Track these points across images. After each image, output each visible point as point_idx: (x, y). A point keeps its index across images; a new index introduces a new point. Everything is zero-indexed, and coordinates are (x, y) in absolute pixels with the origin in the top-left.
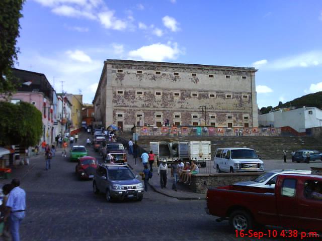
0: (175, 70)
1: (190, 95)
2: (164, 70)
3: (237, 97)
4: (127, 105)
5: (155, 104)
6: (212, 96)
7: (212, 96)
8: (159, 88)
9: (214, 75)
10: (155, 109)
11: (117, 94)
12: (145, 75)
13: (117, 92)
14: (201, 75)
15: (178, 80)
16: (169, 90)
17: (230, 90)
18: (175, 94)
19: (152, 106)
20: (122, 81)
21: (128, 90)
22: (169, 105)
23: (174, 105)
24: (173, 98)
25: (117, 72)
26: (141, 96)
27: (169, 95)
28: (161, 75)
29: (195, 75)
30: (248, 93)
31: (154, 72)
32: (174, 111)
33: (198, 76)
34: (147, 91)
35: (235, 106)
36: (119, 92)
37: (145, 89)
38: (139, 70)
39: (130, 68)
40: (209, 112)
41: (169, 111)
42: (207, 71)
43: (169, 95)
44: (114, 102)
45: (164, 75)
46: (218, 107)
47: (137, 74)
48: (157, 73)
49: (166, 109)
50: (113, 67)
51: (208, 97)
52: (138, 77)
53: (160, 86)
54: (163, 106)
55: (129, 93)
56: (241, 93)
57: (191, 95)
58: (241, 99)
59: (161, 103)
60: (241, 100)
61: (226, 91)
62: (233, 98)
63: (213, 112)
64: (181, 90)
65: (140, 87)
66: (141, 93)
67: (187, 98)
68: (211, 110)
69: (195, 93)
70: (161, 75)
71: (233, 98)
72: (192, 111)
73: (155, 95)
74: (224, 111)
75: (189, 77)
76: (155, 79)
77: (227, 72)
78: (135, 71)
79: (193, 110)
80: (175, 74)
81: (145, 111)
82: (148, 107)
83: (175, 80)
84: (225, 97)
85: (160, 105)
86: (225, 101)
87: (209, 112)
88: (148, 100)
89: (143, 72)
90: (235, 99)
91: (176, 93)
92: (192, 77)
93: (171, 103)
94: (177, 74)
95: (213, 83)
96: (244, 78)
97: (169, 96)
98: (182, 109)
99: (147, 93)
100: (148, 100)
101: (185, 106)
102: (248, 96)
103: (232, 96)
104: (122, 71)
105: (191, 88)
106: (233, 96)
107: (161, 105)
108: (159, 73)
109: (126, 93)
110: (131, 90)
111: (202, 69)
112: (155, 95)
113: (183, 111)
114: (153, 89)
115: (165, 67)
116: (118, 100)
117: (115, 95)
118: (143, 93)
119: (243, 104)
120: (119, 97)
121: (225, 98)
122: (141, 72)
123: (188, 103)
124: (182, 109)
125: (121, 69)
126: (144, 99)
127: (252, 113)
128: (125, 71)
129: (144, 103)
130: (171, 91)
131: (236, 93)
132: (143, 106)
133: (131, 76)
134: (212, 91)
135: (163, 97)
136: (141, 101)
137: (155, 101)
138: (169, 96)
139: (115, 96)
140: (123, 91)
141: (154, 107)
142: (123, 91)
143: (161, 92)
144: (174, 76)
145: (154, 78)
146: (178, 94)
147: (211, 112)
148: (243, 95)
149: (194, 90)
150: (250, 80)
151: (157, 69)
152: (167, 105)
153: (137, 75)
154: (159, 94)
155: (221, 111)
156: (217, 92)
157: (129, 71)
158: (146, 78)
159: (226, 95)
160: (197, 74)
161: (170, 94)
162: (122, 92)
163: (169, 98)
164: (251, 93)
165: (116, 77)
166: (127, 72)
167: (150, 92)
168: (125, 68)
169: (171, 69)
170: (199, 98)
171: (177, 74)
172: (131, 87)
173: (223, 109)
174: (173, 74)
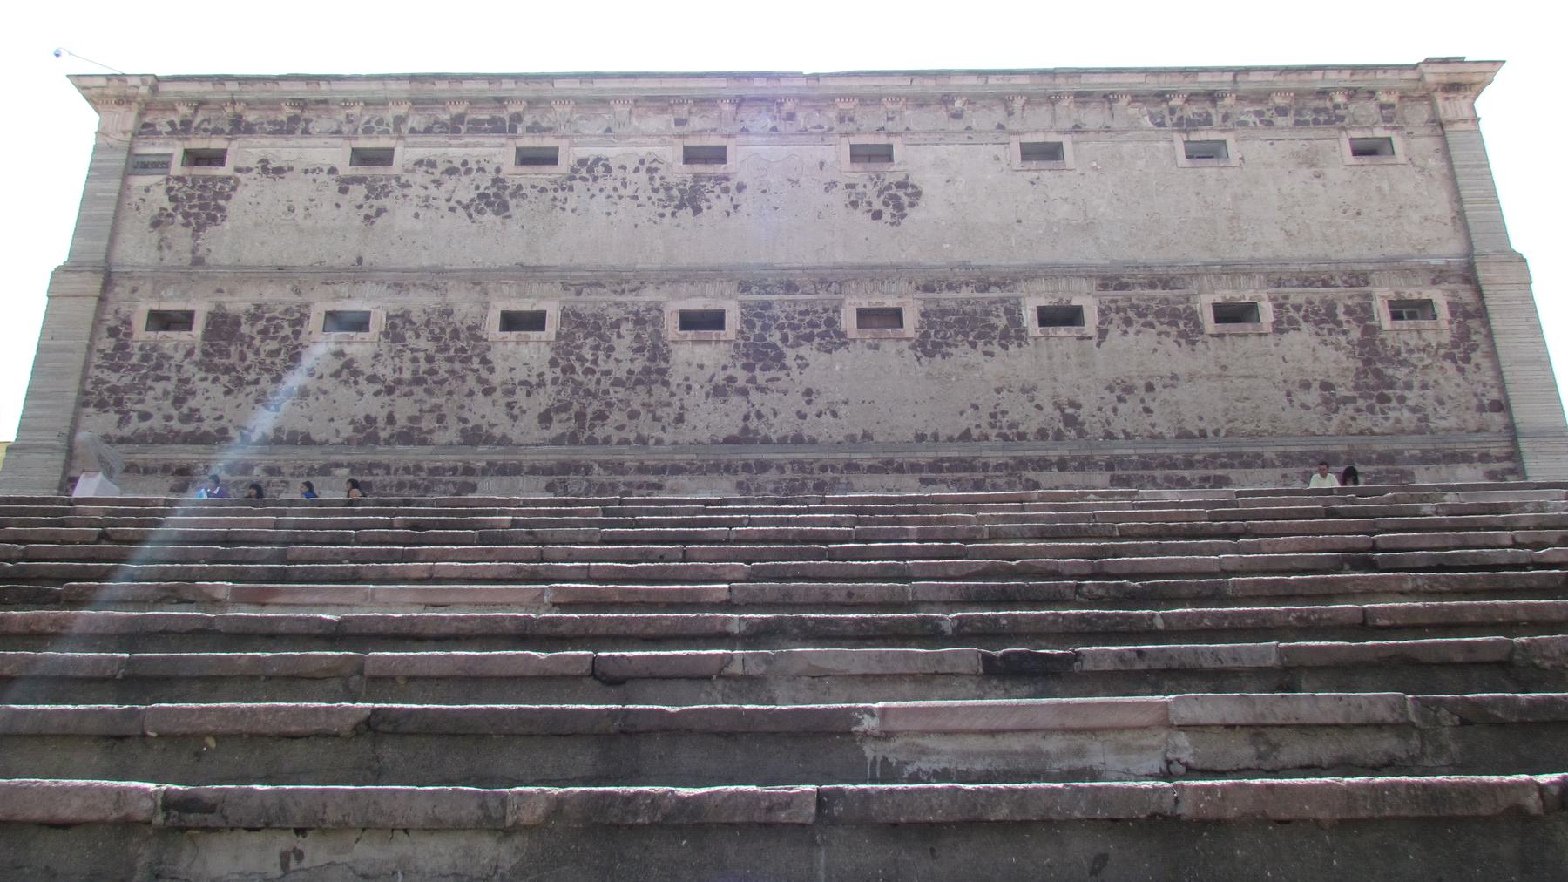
0: (696, 123)
1: (830, 322)
2: (593, 127)
3: (1325, 317)
4: (208, 426)
5: (488, 412)
6: (1060, 316)
7: (1060, 316)
8: (529, 273)
9: (1067, 142)
10: (480, 456)
11: (141, 334)
12: (420, 177)
13: (140, 322)
14: (942, 150)
15: (720, 203)
16: (623, 280)
17: (1243, 253)
18: (690, 321)
19: (452, 434)
20: (212, 230)
21: (239, 303)
22: (616, 417)
23: (668, 414)
24: (658, 352)
25: (177, 169)
26: (360, 347)
27: (626, 328)
28: (563, 167)
29: (885, 154)
30: (1438, 276)
31: (498, 153)
32: (677, 470)
33: (912, 159)
34: (419, 302)
35: (1313, 397)
36: (162, 321)
37: (399, 286)
38: (364, 143)
39: (286, 129)
40: (1042, 465)
41: (618, 468)
42: (999, 115)
43: (626, 328)
44: (101, 405)
45: (590, 168)
46: (1128, 417)
47: (346, 170)
48: (528, 158)
49: (584, 454)
50: (146, 130)
51: (1014, 333)
52: (358, 191)
53: (550, 255)
54: (557, 428)
55: (245, 329)
56: (1358, 278)
57: (848, 321)
58: (1370, 331)
59: (543, 399)
60: (1370, 349)
61: (1195, 274)
62: (1278, 329)
63: (1085, 464)
64: (745, 287)
65: (358, 273)
66: (360, 323)
67: (804, 350)
68: (1064, 451)
69: (890, 302)
70: (563, 167)
71: (1278, 329)
72: (851, 467)
73: (492, 328)
74: (1202, 450)
75: (828, 176)
76: (505, 206)
77: (1191, 111)
78: (337, 155)
79: (863, 457)
80: (691, 156)
81: (379, 477)
82: (406, 437)
83: (691, 200)
84: (1192, 317)
85: (530, 421)
86: (1204, 358)
87: (1042, 465)
88: (417, 381)
89: (405, 154)
90: (1301, 340)
91: (696, 305)
92: (859, 175)
93: (638, 399)
94: (718, 155)
95: (1063, 211)
96: (1365, 150)
97: (623, 344)
98: (753, 454)
99: (418, 317)
100: (417, 381)
101: (782, 426)
102: (1439, 297)
103: (1267, 313)
104: (217, 158)
105: (840, 257)
106: (1279, 306)
107: (545, 418)
108: (550, 158)
109: (222, 327)
110: (276, 295)
111: (946, 100)
112: (492, 328)
113: (763, 467)
114: (478, 279)
115: (604, 101)
116: (140, 389)
117: (122, 347)
118: (378, 323)
119: (1402, 374)
120: (156, 362)
121: (1191, 334)
122: (383, 158)
123: (808, 392)
124: (753, 454)
125: (217, 143)
126: (385, 371)
127: (1514, 455)
128: (243, 152)
129: (371, 404)
130: (649, 295)
131: (1306, 281)
132: (366, 432)
133: (294, 189)
134: (1052, 272)
135: (564, 349)
136: (344, 394)
137: (488, 391)
138: (623, 344)
139: (118, 355)
140: (201, 308)
141: (473, 437)
142: (201, 308)
143: (553, 310)
144: (677, 171)
145: (496, 199)
146: (714, 320)
147: (1062, 465)
148: (1382, 294)
149: (877, 274)
150: (1435, 163)
151: (534, 129)
152: (601, 416)
153: (344, 186)
154: (536, 321)
155: (1176, 450)
156: (1109, 280)
157: (283, 151)
158: (427, 203)
159: (1204, 305)
160: (897, 143)
161: (639, 321)
162: (183, 321)
163: (624, 356)
164: (1469, 276)
165: (160, 199)
166: (264, 163)
167: (448, 313)
168: (250, 130)
169: (656, 122)
170: (928, 346)
171: (718, 155)
172: (282, 272)
173: (1184, 436)
174: (672, 155)
